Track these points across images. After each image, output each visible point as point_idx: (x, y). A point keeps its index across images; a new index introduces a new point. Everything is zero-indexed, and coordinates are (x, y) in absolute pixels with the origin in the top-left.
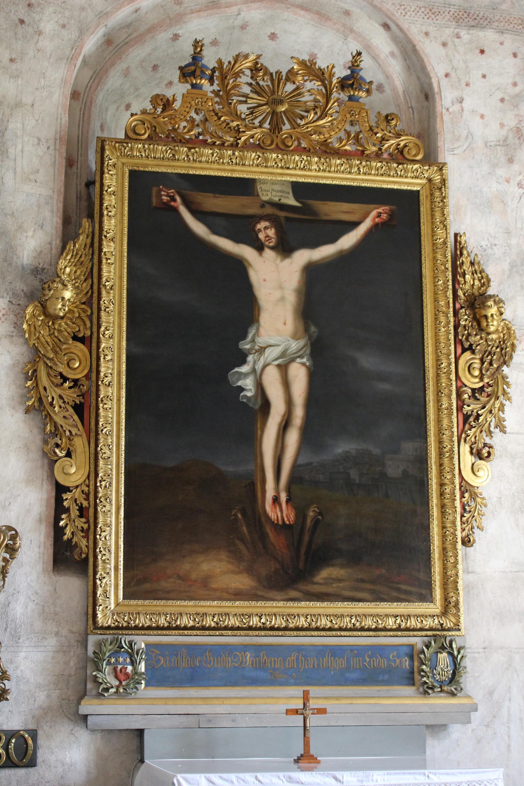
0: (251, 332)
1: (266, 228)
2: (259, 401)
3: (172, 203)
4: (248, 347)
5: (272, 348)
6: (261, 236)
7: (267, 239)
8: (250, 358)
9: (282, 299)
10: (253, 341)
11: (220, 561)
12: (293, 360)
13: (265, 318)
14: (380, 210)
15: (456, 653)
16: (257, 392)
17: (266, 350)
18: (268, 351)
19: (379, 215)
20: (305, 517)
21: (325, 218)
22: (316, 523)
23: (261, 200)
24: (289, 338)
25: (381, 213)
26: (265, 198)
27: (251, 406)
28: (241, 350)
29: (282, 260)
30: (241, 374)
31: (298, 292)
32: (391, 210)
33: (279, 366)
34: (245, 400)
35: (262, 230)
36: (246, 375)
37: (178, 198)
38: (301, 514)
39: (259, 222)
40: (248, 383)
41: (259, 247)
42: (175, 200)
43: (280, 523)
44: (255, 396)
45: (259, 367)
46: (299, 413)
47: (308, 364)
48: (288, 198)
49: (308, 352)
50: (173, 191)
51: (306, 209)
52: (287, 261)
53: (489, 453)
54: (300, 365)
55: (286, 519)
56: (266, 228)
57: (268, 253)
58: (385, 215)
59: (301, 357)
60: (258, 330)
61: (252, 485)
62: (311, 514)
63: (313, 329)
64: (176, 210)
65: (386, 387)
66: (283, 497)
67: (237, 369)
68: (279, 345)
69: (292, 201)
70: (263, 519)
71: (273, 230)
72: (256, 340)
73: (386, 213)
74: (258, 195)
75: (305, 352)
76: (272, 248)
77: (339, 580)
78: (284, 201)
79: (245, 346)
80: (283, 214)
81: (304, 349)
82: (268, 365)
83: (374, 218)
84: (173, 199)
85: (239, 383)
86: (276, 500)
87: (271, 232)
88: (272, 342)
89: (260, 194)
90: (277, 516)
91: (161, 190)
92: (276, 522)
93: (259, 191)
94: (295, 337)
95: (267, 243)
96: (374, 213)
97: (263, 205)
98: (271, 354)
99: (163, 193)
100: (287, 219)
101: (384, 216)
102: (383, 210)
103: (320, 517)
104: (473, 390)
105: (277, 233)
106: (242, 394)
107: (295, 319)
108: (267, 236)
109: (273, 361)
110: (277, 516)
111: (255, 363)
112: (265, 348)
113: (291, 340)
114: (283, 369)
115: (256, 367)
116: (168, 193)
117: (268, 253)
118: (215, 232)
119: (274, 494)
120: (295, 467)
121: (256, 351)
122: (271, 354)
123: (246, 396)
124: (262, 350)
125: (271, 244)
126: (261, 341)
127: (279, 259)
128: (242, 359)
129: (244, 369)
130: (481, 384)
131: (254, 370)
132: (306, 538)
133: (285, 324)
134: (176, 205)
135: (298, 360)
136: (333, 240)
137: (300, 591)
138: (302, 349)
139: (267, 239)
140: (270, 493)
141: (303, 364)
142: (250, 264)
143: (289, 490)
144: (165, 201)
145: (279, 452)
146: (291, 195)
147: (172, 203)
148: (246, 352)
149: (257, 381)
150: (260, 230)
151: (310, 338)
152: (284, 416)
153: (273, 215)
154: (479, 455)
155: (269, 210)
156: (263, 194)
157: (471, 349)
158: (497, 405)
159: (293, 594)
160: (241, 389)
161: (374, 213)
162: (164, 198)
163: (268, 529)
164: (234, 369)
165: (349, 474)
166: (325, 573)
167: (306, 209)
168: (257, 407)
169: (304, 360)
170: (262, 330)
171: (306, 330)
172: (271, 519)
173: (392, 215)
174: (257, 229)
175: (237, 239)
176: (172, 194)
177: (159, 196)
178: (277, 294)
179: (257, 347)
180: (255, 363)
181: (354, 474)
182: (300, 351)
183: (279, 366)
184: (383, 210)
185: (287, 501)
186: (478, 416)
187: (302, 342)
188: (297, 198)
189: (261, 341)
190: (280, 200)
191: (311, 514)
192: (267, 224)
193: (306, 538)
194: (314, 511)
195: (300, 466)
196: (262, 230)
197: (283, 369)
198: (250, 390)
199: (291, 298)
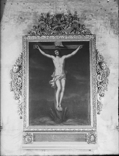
0: (54, 73)
1: (57, 52)
3: (38, 48)
6: (56, 53)
8: (53, 79)
10: (54, 75)
11: (48, 118)
12: (62, 78)
15: (95, 136)
18: (57, 77)
19: (81, 47)
20: (65, 109)
21: (69, 48)
22: (67, 110)
30: (51, 82)
31: (63, 64)
32: (83, 46)
33: (59, 80)
36: (52, 82)
37: (39, 47)
38: (64, 108)
40: (53, 84)
41: (55, 56)
42: (38, 48)
44: (54, 86)
45: (55, 80)
46: (63, 89)
51: (65, 47)
52: (61, 58)
53: (103, 95)
56: (57, 52)
57: (57, 57)
59: (64, 78)
60: (55, 73)
61: (54, 104)
62: (66, 109)
63: (66, 72)
64: (38, 50)
65: (82, 83)
66: (60, 106)
67: (51, 81)
69: (62, 46)
70: (56, 110)
76: (58, 56)
77: (71, 122)
78: (60, 46)
80: (60, 48)
82: (57, 80)
84: (38, 47)
86: (59, 106)
87: (58, 52)
89: (55, 45)
91: (35, 46)
94: (62, 74)
96: (79, 47)
97: (56, 47)
100: (61, 49)
101: (82, 47)
104: (100, 82)
105: (59, 53)
111: (54, 79)
114: (60, 80)
117: (57, 57)
118: (46, 53)
120: (63, 99)
126: (56, 75)
129: (52, 81)
130: (102, 81)
131: (54, 81)
132: (65, 113)
135: (63, 78)
136: (71, 53)
137: (63, 124)
141: (64, 79)
142: (53, 59)
143: (61, 104)
146: (62, 44)
147: (38, 48)
151: (66, 74)
153: (58, 49)
154: (101, 96)
155: (57, 48)
157: (100, 74)
158: (106, 85)
159: (62, 124)
160: (52, 85)
161: (79, 47)
163: (57, 113)
165: (74, 101)
166: (69, 120)
167: (65, 47)
168: (55, 88)
170: (56, 73)
171: (65, 72)
172: (58, 111)
173: (83, 47)
175: (51, 55)
177: (35, 47)
178: (59, 65)
180: (54, 79)
181: (75, 101)
183: (59, 80)
185: (61, 107)
186: (101, 87)
187: (64, 75)
188: (63, 45)
191: (66, 109)
193: (65, 113)
197: (60, 80)
199: (62, 66)
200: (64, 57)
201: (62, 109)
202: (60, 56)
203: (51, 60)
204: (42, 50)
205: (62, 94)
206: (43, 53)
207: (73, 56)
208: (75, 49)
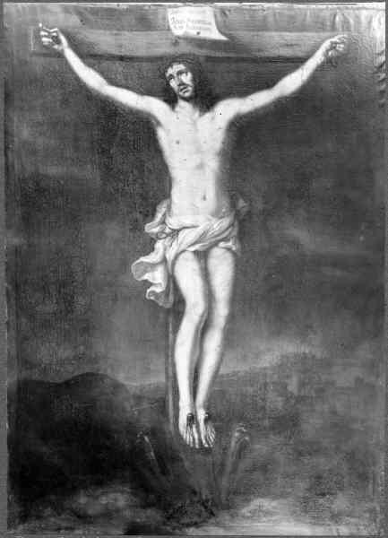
0: (161, 210)
1: (180, 73)
2: (171, 298)
3: (56, 47)
4: (156, 230)
5: (187, 231)
6: (174, 84)
7: (182, 87)
8: (159, 245)
9: (201, 166)
10: (163, 222)
12: (216, 244)
13: (178, 195)
14: (335, 39)
16: (168, 287)
17: (181, 233)
18: (181, 235)
19: (333, 46)
21: (262, 54)
23: (172, 34)
24: (210, 217)
25: (336, 43)
26: (178, 32)
27: (161, 304)
28: (148, 234)
29: (200, 116)
33: (196, 253)
34: (152, 298)
35: (175, 75)
36: (153, 266)
37: (63, 38)
39: (171, 65)
40: (157, 278)
41: (171, 99)
43: (197, 446)
44: (166, 293)
45: (170, 255)
46: (222, 311)
47: (234, 249)
48: (208, 29)
49: (235, 233)
50: (56, 29)
52: (208, 115)
54: (224, 250)
55: (204, 442)
56: (180, 73)
58: (342, 46)
60: (169, 208)
63: (241, 203)
64: (60, 55)
66: (201, 415)
67: (143, 259)
68: (194, 227)
71: (190, 75)
72: (167, 222)
73: (343, 43)
74: (169, 29)
75: (230, 233)
78: (205, 35)
79: (152, 228)
81: (230, 229)
82: (183, 251)
83: (327, 51)
84: (58, 41)
85: (146, 277)
86: (192, 419)
87: (187, 79)
88: (188, 222)
89: (172, 26)
90: (194, 439)
92: (192, 445)
93: (171, 22)
94: (217, 214)
95: (181, 93)
96: (327, 44)
97: (176, 41)
98: (187, 237)
99: (43, 33)
100: (208, 59)
102: (339, 39)
103: (247, 438)
105: (194, 80)
106: (148, 291)
107: (217, 195)
108: (182, 84)
109: (189, 246)
110: (194, 439)
112: (178, 231)
113: (214, 220)
115: (167, 256)
116: (49, 33)
118: (112, 82)
119: (189, 412)
120: (216, 376)
121: (168, 235)
122: (187, 237)
123: (153, 293)
124: (175, 233)
125: (187, 95)
126: (173, 223)
127: (197, 114)
128: (149, 247)
129: (153, 258)
131: (164, 260)
133: (204, 198)
134: (60, 48)
135: (222, 244)
136: (269, 84)
138: (227, 229)
139: (182, 87)
140: (185, 412)
141: (229, 249)
142: (159, 123)
144: (46, 44)
145: (195, 358)
146: (214, 27)
147: (56, 47)
148: (154, 237)
149: (168, 274)
150: (171, 77)
151: (237, 215)
152: (202, 316)
155: (184, 48)
156: (175, 27)
160: (148, 284)
162: (44, 39)
164: (138, 259)
169: (230, 244)
170: (175, 209)
171: (233, 205)
174: (167, 75)
176: (55, 34)
177: (38, 37)
178: (196, 160)
179: (167, 231)
182: (223, 232)
183: (196, 253)
184: (339, 39)
185: (206, 421)
187: (226, 222)
189: (173, 223)
190: (198, 33)
191: (237, 434)
192: (181, 67)
194: (240, 431)
195: (222, 376)
196: (175, 75)
197: (202, 256)
198: (160, 284)
199: (213, 164)
200: (229, 109)
201: (212, 437)
202: (205, 99)
203: (145, 127)
204: (91, 57)
205: (214, 342)
206: (92, 78)
207: (281, 106)
208: (297, 62)
